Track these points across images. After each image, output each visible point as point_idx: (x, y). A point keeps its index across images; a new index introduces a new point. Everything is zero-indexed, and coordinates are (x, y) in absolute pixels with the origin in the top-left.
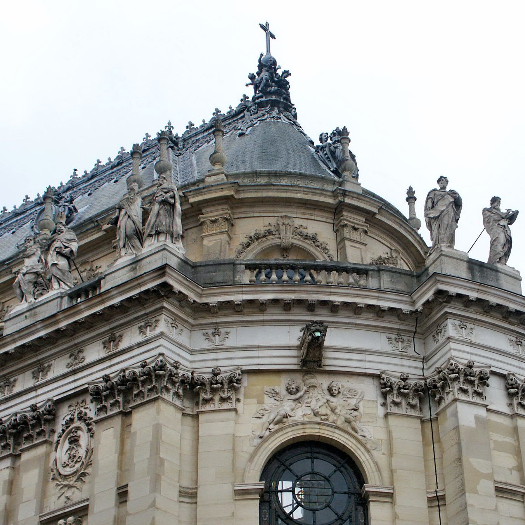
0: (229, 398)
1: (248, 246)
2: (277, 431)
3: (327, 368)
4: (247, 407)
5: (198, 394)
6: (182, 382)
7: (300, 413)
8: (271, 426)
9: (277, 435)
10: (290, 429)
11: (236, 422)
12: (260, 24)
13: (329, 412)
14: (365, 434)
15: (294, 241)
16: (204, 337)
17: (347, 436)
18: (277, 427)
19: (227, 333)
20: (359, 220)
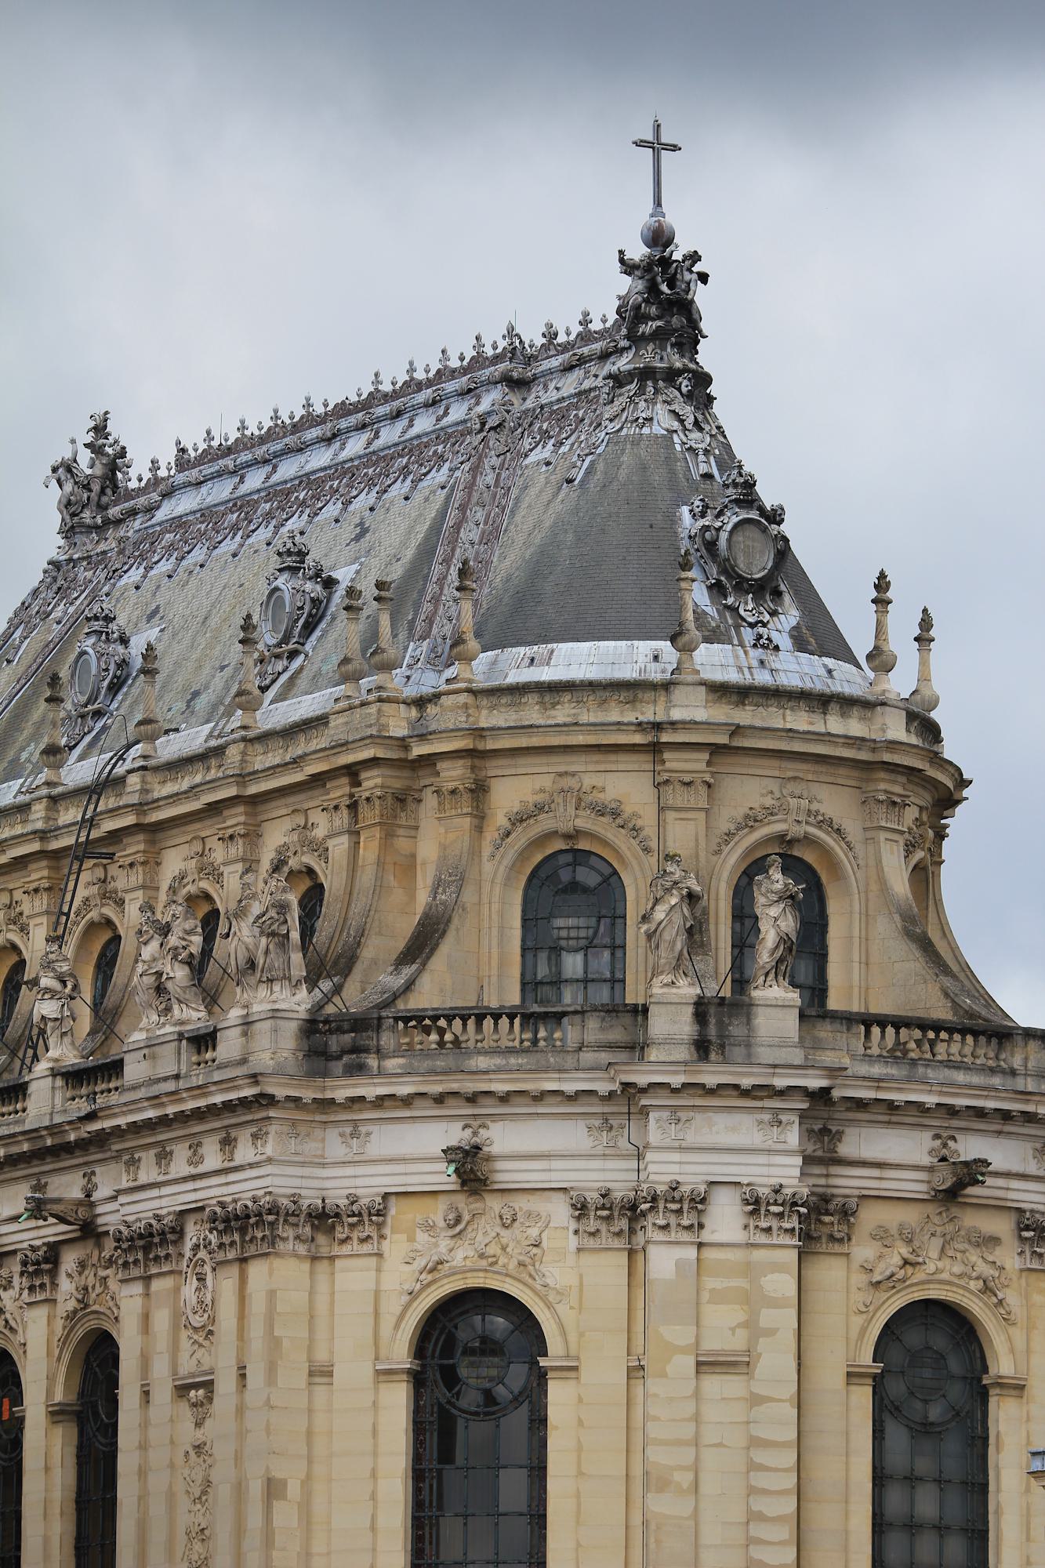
0: (369, 1237)
1: (508, 834)
2: (429, 1285)
3: (496, 1187)
4: (395, 1246)
5: (333, 1227)
6: (310, 1215)
7: (462, 1255)
8: (423, 1277)
9: (429, 1290)
10: (446, 1281)
11: (379, 1270)
12: (635, 143)
13: (499, 1252)
14: (549, 1281)
15: (580, 823)
16: (340, 1139)
17: (521, 1286)
18: (430, 1277)
19: (368, 1134)
20: (696, 762)
